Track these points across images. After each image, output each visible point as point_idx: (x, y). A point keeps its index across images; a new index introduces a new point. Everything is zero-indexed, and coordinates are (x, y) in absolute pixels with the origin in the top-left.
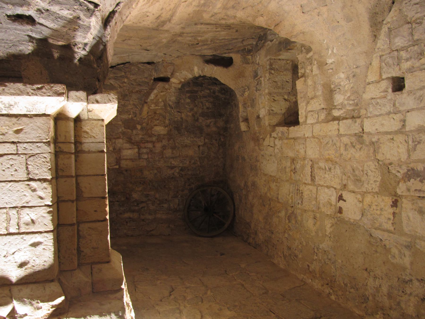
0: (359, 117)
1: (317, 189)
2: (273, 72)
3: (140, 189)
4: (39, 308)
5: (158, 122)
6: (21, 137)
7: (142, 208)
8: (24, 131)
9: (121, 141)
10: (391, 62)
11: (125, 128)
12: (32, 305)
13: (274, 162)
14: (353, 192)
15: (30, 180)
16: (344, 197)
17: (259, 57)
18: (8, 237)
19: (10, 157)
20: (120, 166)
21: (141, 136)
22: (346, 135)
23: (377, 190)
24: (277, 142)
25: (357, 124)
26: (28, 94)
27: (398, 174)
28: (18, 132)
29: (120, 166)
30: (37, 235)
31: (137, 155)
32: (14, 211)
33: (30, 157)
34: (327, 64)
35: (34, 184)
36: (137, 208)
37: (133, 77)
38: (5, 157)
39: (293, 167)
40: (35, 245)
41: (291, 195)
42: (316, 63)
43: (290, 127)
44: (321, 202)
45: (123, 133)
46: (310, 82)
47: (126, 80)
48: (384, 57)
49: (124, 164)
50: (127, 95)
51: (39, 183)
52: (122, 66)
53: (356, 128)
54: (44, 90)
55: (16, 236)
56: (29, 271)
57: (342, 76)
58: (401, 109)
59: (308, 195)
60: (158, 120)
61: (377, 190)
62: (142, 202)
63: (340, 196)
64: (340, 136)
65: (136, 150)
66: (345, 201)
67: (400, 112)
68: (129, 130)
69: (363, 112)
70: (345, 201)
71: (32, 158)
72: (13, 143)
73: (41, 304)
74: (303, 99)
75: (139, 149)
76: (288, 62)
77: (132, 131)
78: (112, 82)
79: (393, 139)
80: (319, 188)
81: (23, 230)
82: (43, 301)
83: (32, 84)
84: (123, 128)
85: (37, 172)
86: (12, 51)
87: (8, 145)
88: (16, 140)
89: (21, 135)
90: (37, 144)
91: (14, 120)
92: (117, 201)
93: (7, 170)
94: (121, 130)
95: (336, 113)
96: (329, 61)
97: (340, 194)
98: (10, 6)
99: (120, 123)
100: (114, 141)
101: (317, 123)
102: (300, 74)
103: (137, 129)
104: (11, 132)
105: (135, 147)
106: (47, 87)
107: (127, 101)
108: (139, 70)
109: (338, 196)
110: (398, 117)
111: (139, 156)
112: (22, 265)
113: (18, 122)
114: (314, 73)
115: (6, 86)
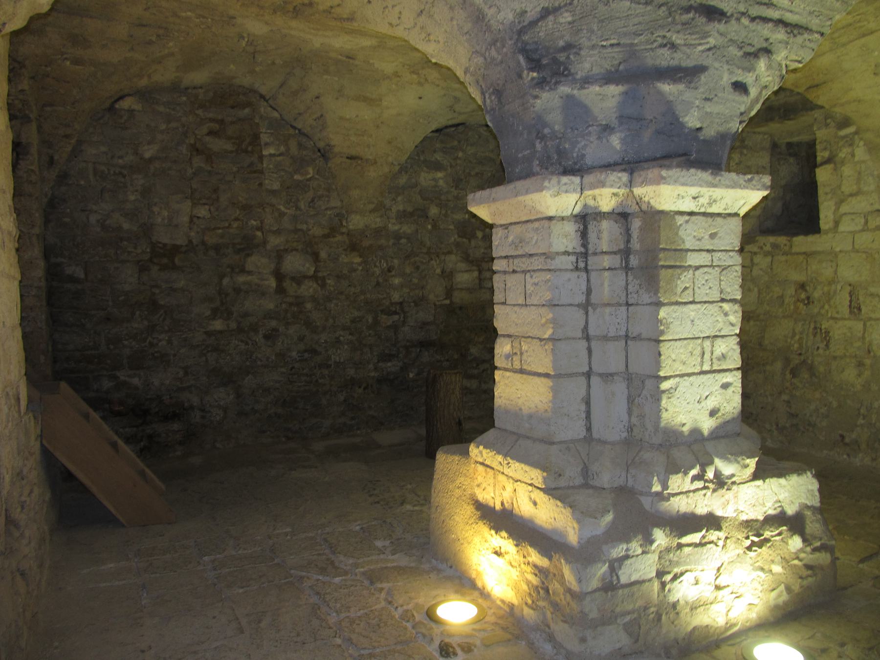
1: (865, 325)
2: (745, 151)
3: (481, 339)
4: (746, 466)
6: (717, 244)
7: (483, 371)
8: (719, 235)
9: (453, 257)
11: (459, 236)
12: (738, 463)
15: (723, 300)
18: (702, 376)
19: (706, 269)
20: (451, 301)
21: (482, 250)
24: (757, 259)
26: (741, 187)
28: (713, 236)
29: (451, 302)
30: (727, 373)
31: (477, 281)
32: (707, 344)
33: (723, 270)
35: (726, 306)
36: (476, 372)
37: (471, 150)
38: (702, 270)
39: (803, 296)
40: (725, 386)
41: (797, 337)
42: (862, 143)
43: (796, 234)
45: (457, 245)
46: (847, 170)
47: (460, 154)
49: (459, 297)
50: (462, 180)
51: (731, 304)
52: (453, 129)
54: (754, 182)
55: (709, 376)
56: (719, 421)
59: (844, 334)
62: (484, 361)
65: (476, 274)
68: (464, 240)
71: (724, 272)
72: (708, 251)
73: (748, 461)
74: (829, 196)
75: (480, 272)
76: (766, 137)
77: (470, 241)
78: (438, 156)
80: (868, 324)
81: (715, 367)
82: (748, 458)
83: (745, 174)
84: (456, 236)
85: (729, 290)
86: (722, 129)
87: (704, 254)
88: (711, 248)
89: (716, 241)
90: (731, 253)
91: (710, 220)
92: (447, 360)
93: (702, 288)
94: (453, 239)
98: (740, 71)
99: (452, 227)
100: (443, 257)
101: (863, 230)
102: (819, 159)
103: (477, 237)
104: (707, 237)
105: (475, 268)
106: (756, 177)
107: (462, 189)
108: (480, 137)
111: (480, 284)
112: (713, 413)
113: (714, 223)
114: (856, 159)
115: (722, 176)
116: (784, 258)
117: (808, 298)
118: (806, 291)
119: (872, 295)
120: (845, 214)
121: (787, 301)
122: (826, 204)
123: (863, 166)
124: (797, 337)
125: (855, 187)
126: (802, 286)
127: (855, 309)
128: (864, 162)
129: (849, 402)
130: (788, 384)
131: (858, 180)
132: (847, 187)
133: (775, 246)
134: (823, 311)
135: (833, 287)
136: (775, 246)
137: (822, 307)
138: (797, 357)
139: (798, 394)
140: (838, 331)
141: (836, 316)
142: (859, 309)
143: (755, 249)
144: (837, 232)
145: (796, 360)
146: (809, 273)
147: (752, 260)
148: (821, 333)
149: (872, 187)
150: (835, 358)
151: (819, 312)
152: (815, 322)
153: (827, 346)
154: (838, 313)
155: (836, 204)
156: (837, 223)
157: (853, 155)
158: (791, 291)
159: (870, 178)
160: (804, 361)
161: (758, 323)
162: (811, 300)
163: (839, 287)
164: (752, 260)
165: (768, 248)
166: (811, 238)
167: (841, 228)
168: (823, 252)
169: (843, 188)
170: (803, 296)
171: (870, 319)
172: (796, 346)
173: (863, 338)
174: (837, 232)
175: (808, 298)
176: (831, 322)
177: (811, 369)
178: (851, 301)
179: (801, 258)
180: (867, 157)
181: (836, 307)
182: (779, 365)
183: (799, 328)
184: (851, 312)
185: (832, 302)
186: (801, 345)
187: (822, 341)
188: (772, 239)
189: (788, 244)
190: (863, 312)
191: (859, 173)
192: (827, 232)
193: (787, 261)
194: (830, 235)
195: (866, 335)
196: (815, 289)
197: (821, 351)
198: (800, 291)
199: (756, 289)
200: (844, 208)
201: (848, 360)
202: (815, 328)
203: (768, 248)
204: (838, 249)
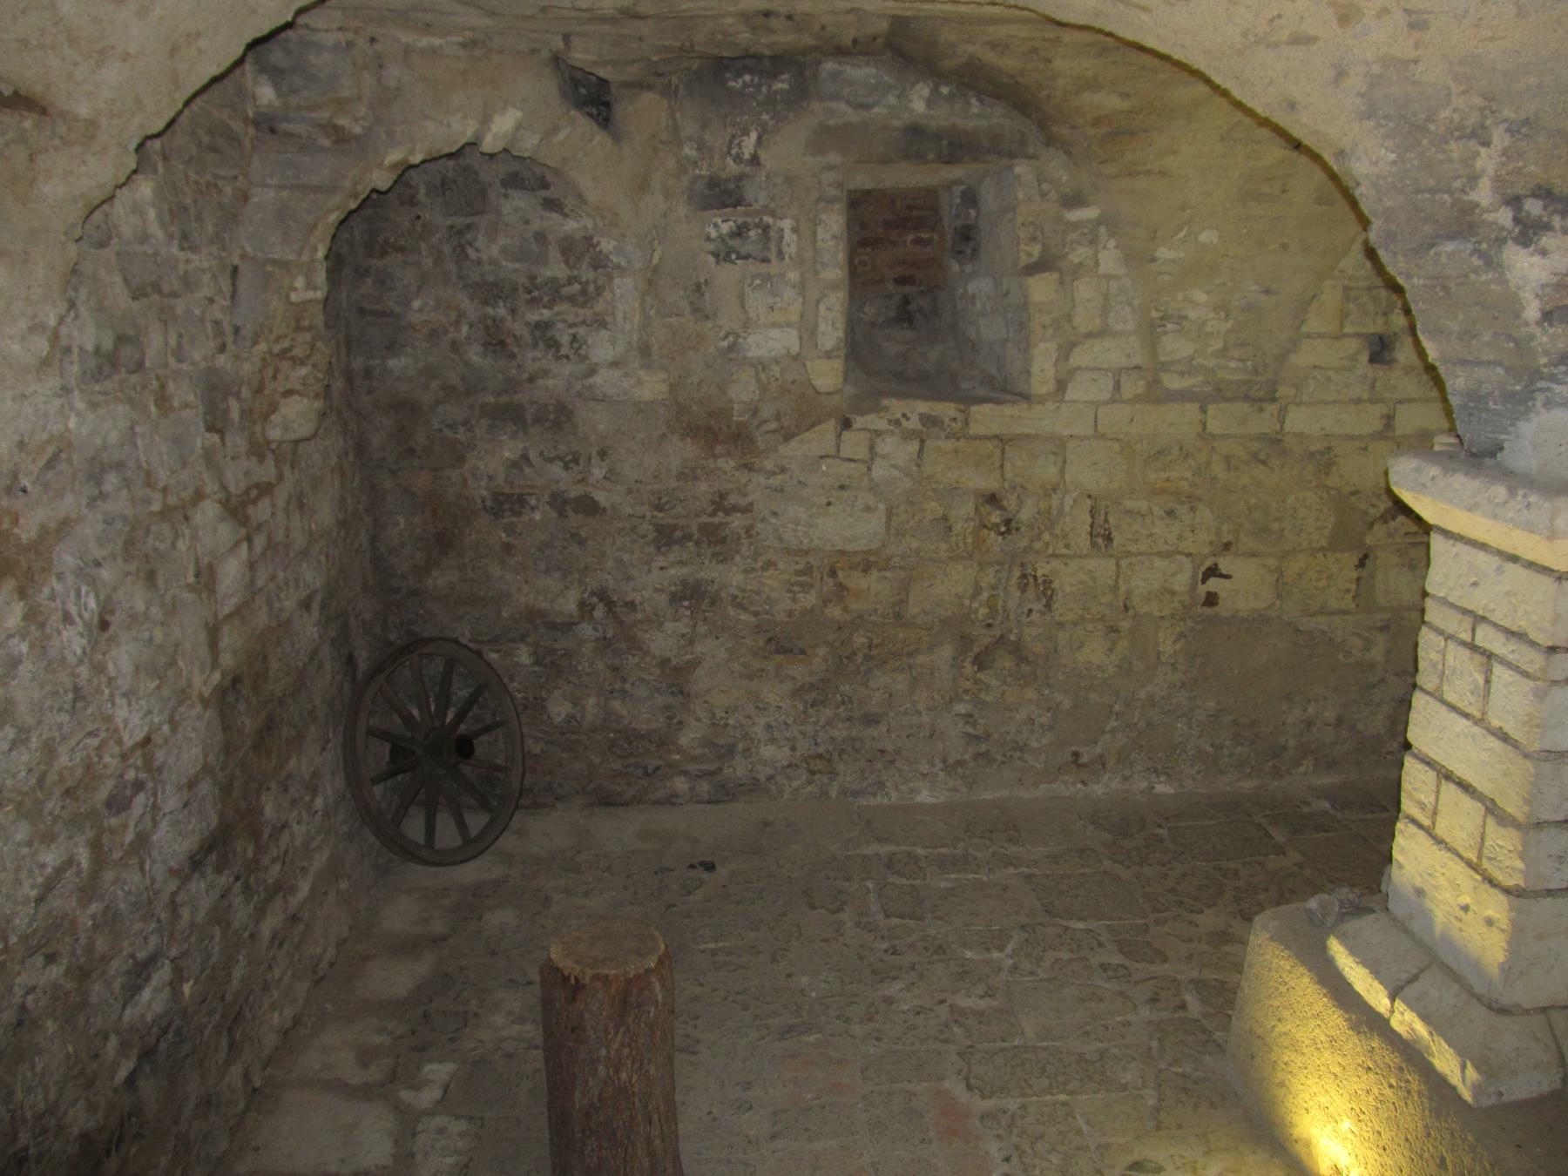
0: (1274, 400)
1: (1118, 565)
5: (304, 371)
10: (1371, 307)
13: (868, 509)
14: (1254, 555)
16: (1224, 569)
17: (759, 139)
22: (1224, 437)
23: (1324, 543)
24: (887, 446)
25: (1266, 415)
27: (1372, 511)
34: (1154, 260)
41: (985, 595)
42: (1112, 243)
44: (1137, 592)
46: (1084, 290)
48: (1353, 293)
53: (1264, 422)
57: (1200, 296)
58: (1387, 395)
59: (1082, 582)
60: (303, 363)
61: (1324, 543)
63: (1209, 569)
64: (1205, 435)
66: (1227, 577)
67: (1382, 401)
69: (1284, 391)
70: (1227, 577)
74: (1050, 332)
79: (1365, 449)
80: (1124, 563)
95: (1173, 382)
96: (1163, 253)
97: (1209, 563)
101: (1113, 401)
109: (1203, 569)
110: (1379, 409)
114: (1102, 270)
116: (949, 445)
117: (1008, 522)
118: (1003, 508)
119: (1129, 512)
120: (1079, 368)
121: (958, 528)
122: (1042, 346)
123: (1114, 285)
124: (985, 595)
125: (1098, 321)
126: (993, 499)
127: (1102, 537)
128: (1116, 277)
129: (1092, 696)
130: (968, 685)
131: (1105, 312)
132: (1084, 320)
133: (929, 421)
134: (1038, 545)
135: (1055, 501)
136: (929, 421)
137: (1039, 537)
138: (985, 631)
139: (989, 698)
140: (1067, 578)
141: (1066, 551)
142: (1108, 539)
143: (881, 424)
144: (1062, 401)
145: (985, 638)
146: (1009, 475)
147: (872, 448)
148: (1037, 585)
149: (1131, 326)
150: (1061, 625)
151: (1030, 547)
152: (1022, 565)
153: (1048, 606)
154: (1067, 546)
155: (1060, 347)
156: (1061, 385)
157: (1097, 264)
158: (963, 512)
159: (1128, 310)
160: (1002, 637)
161: (888, 574)
162: (1014, 525)
163: (1069, 501)
164: (872, 448)
165: (914, 424)
166: (1008, 410)
167: (1070, 394)
168: (1036, 436)
169: (1077, 321)
170: (996, 518)
171: (1128, 554)
172: (983, 611)
173: (1115, 588)
174: (1062, 401)
175: (1008, 522)
176: (1055, 563)
177: (1018, 651)
178: (1091, 526)
179: (990, 446)
180: (1122, 271)
181: (1065, 537)
182: (946, 652)
183: (989, 578)
184: (1094, 545)
185: (1057, 531)
186: (993, 610)
187: (1038, 599)
188: (923, 407)
189: (960, 417)
190: (1115, 544)
191: (1106, 297)
192: (1042, 400)
193: (956, 451)
194: (1050, 406)
195: (1121, 582)
196: (1021, 504)
197: (1035, 616)
198: (988, 508)
199: (882, 507)
200: (1078, 358)
201: (1090, 627)
202: (1024, 576)
203: (914, 424)
204: (1066, 433)
